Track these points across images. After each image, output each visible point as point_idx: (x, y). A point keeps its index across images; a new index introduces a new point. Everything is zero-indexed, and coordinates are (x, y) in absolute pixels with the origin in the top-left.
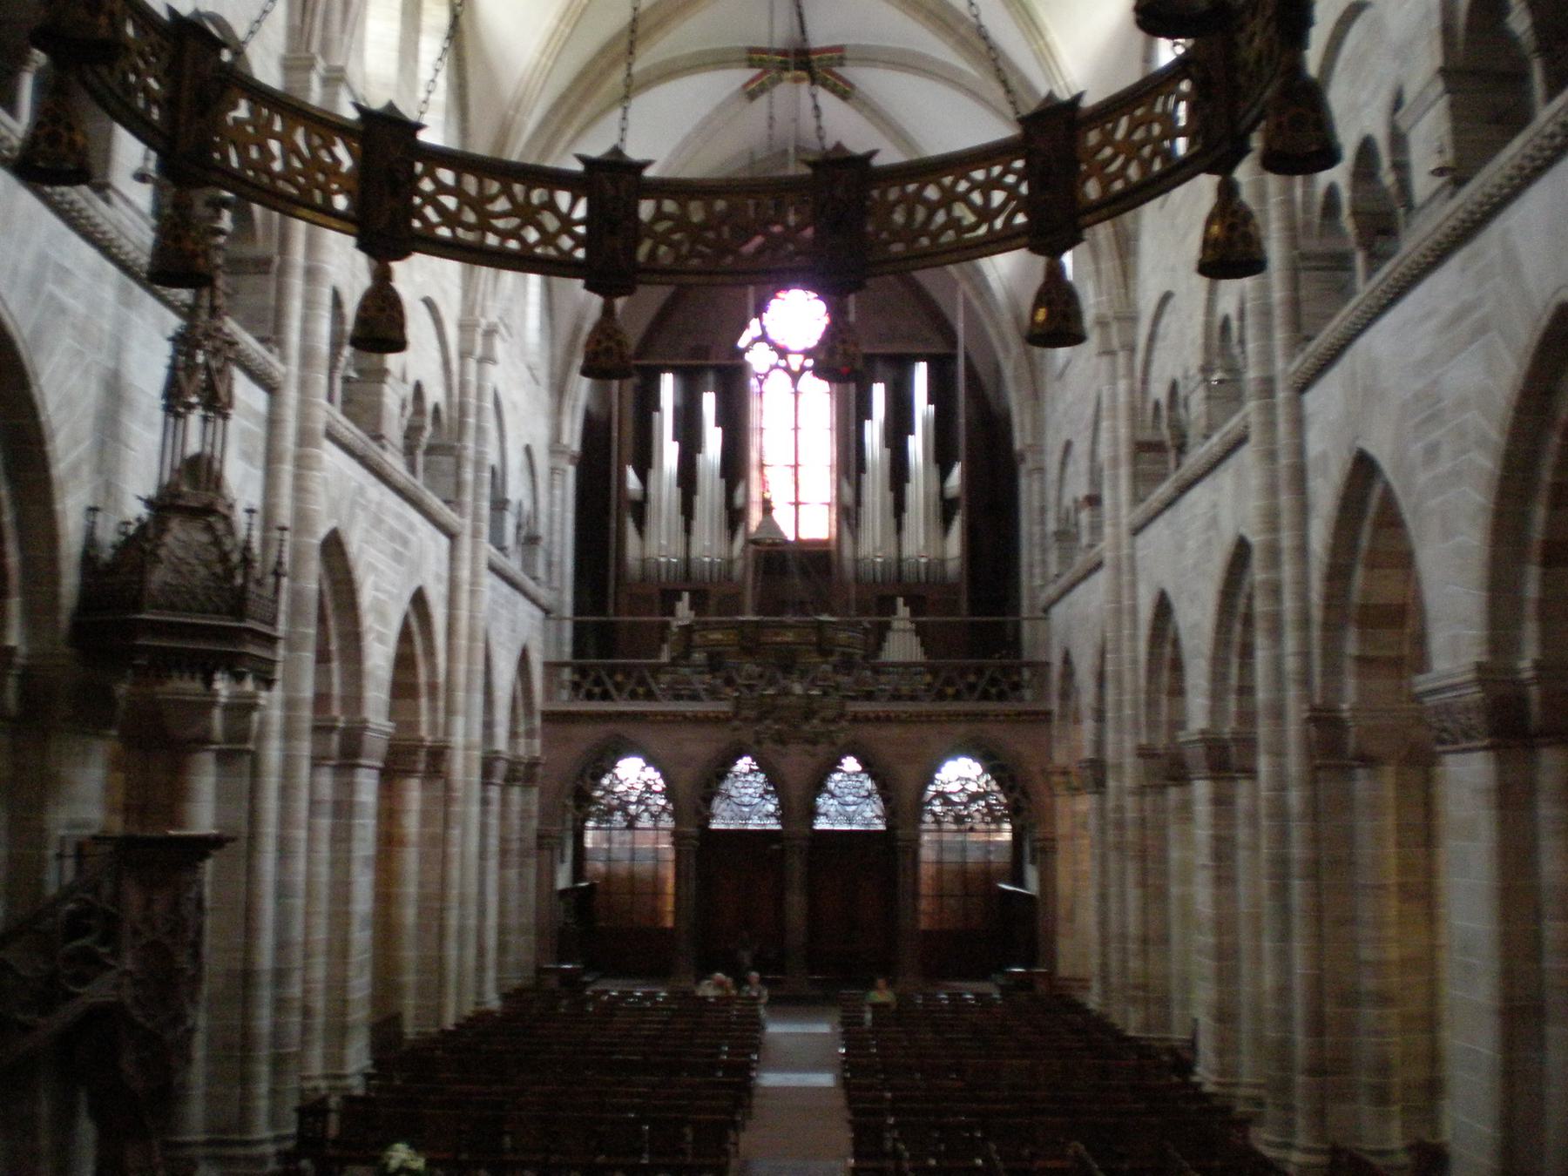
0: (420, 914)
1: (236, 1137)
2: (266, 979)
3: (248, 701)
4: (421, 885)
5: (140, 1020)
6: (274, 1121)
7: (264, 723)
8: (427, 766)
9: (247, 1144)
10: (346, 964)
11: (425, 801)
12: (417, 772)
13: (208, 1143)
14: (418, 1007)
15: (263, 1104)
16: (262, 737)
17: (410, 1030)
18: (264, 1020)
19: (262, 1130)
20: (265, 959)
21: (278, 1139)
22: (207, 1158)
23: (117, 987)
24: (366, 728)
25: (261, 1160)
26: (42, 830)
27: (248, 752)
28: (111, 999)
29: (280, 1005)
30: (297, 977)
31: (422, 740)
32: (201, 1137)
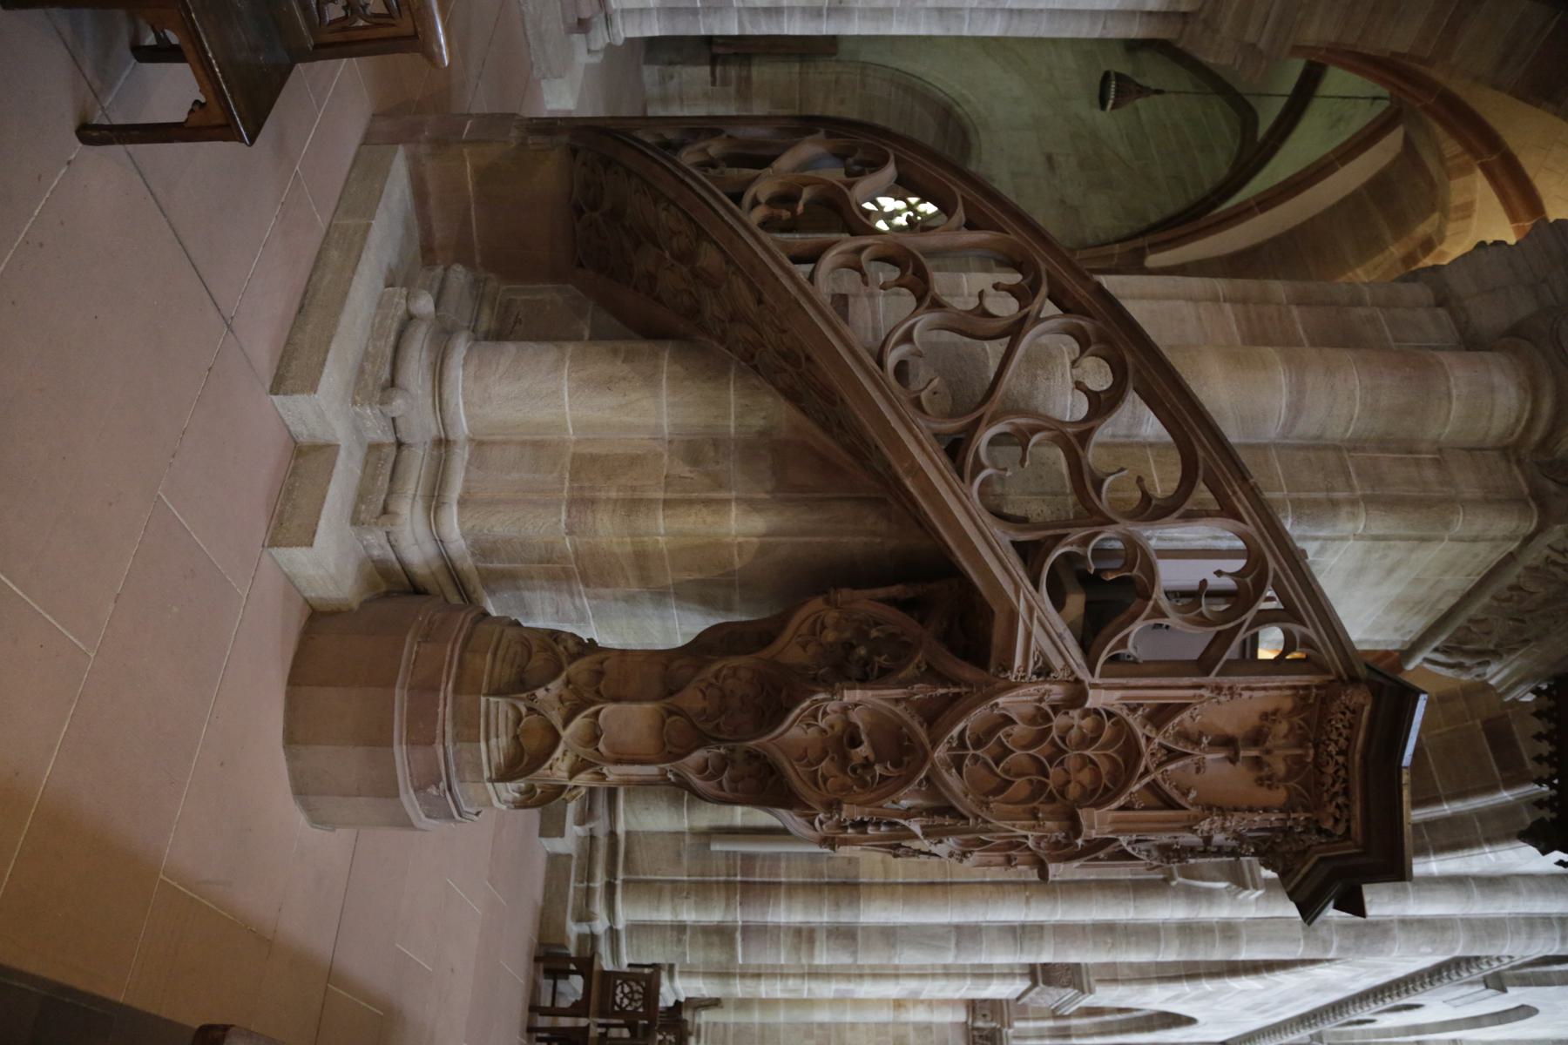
0: (821, 1025)
1: (621, 876)
2: (845, 917)
3: (1248, 876)
4: (853, 1026)
5: (955, 732)
6: (636, 928)
7: (1210, 893)
8: (978, 1029)
9: (610, 888)
10: (802, 976)
11: (941, 1026)
12: (974, 1019)
13: (612, 834)
14: (725, 1025)
15: (665, 915)
16: (1192, 894)
17: (704, 1017)
18: (785, 914)
19: (625, 914)
20: (874, 914)
21: (613, 933)
22: (592, 838)
23: (1045, 671)
24: (1083, 992)
25: (585, 916)
26: (1334, 504)
27: (1166, 881)
28: (1018, 661)
29: (804, 936)
30: (844, 959)
31: (1010, 1026)
32: (621, 829)
